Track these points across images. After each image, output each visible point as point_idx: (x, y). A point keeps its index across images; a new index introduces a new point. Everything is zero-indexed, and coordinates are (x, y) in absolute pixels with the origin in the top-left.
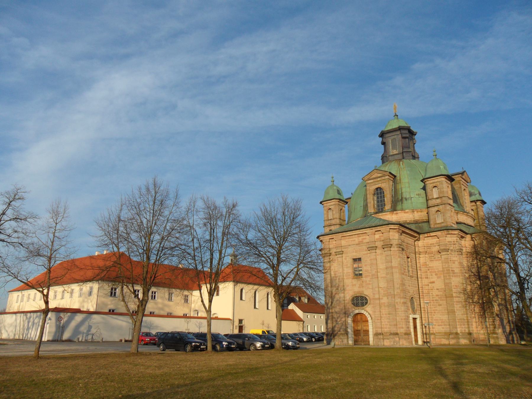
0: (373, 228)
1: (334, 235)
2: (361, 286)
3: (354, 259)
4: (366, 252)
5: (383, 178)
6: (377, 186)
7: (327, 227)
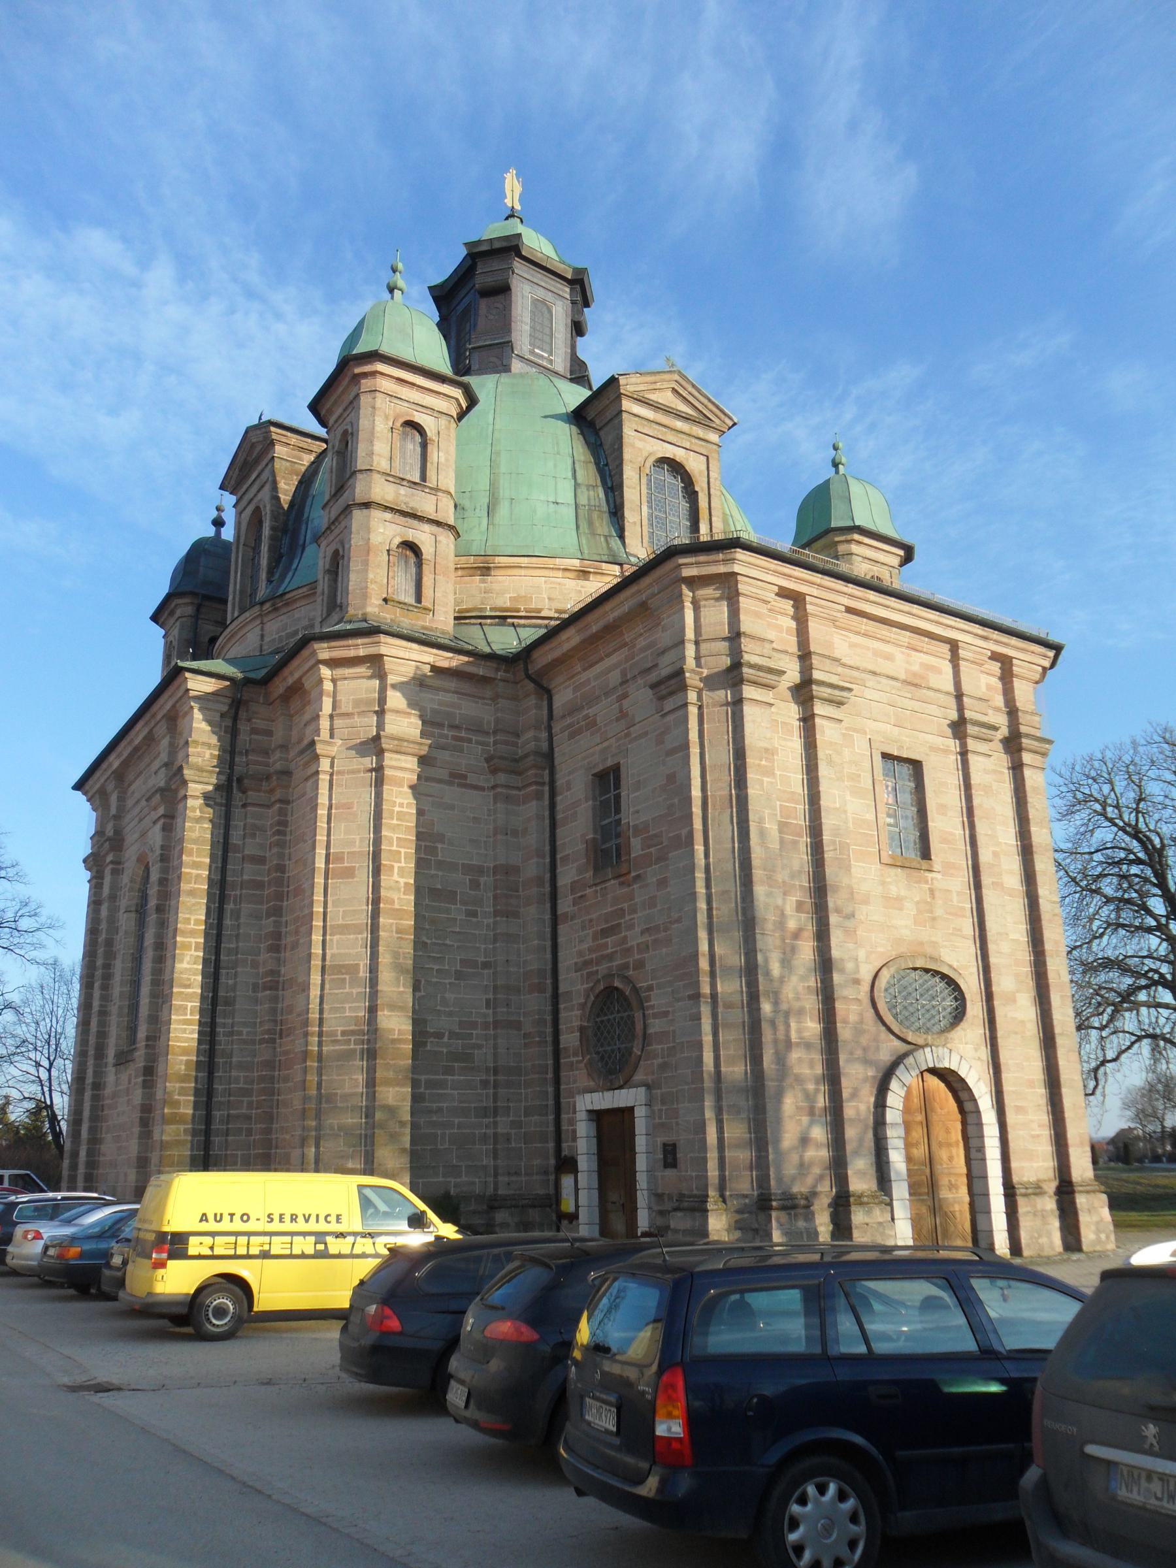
0: (995, 635)
1: (817, 578)
2: (927, 914)
3: (885, 756)
4: (940, 741)
5: (699, 431)
6: (670, 451)
7: (388, 516)
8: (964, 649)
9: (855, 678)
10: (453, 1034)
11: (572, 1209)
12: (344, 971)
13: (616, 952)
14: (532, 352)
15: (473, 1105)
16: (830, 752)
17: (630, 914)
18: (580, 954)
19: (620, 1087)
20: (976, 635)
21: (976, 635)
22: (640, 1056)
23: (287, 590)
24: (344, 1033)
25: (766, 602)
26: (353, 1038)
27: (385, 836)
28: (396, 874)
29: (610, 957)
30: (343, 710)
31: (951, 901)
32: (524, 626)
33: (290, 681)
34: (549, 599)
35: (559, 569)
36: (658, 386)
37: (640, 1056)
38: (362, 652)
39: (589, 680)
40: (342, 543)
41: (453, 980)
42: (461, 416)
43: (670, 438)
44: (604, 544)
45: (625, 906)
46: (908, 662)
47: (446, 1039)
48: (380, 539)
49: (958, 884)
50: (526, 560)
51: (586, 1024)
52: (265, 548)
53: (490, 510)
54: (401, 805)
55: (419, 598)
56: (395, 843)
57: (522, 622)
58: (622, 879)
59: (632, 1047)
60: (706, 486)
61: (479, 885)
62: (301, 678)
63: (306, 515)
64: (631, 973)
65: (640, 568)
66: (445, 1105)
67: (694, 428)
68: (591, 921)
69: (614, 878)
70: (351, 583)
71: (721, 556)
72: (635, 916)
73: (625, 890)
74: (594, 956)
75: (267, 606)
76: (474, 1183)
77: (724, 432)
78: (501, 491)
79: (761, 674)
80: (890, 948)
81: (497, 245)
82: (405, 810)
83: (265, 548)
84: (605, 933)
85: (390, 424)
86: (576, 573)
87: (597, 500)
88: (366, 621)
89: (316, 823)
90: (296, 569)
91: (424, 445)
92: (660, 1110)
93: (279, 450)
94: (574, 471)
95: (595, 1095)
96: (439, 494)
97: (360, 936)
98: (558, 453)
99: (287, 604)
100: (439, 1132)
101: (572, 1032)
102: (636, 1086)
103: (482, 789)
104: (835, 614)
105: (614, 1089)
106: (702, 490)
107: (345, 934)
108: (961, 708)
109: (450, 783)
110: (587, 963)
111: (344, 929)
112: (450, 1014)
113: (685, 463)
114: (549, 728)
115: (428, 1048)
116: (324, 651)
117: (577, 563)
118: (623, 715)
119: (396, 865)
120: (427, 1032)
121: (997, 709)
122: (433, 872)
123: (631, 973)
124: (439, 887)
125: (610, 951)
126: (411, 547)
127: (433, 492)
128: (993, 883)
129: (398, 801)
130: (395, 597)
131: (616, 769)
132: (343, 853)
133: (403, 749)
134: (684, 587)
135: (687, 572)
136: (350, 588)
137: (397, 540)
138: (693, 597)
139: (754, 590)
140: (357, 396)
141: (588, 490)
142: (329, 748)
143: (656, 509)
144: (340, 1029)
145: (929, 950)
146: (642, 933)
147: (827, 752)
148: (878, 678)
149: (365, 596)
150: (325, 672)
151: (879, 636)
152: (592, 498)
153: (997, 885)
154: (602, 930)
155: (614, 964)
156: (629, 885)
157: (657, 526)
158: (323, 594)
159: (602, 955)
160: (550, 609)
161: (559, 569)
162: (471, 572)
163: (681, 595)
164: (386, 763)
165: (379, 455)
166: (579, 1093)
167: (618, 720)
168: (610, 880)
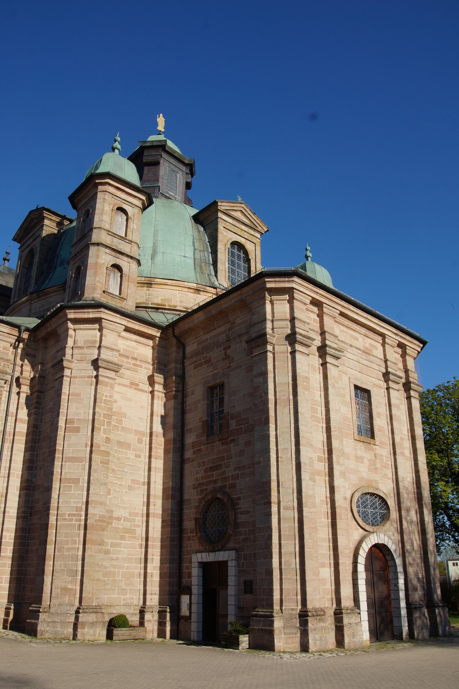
1: (329, 296)
4: (377, 382)
7: (108, 251)
8: (388, 339)
9: (343, 347)
10: (126, 519)
11: (188, 614)
12: (71, 482)
13: (219, 479)
14: (167, 193)
15: (134, 557)
16: (334, 382)
17: (227, 460)
18: (196, 479)
19: (219, 550)
20: (393, 332)
21: (393, 332)
22: (232, 534)
23: (47, 287)
24: (69, 515)
25: (306, 304)
26: (74, 518)
27: (98, 412)
28: (101, 432)
29: (215, 482)
30: (79, 344)
31: (383, 460)
32: (168, 313)
33: (49, 329)
34: (180, 301)
35: (186, 287)
36: (235, 208)
37: (232, 534)
38: (91, 316)
39: (207, 339)
40: (83, 263)
41: (127, 490)
42: (144, 208)
43: (239, 232)
44: (207, 278)
45: (225, 455)
46: (364, 342)
47: (122, 521)
48: (103, 261)
49: (386, 451)
50: (170, 281)
51: (199, 517)
52: (35, 268)
53: (153, 256)
54: (106, 396)
55: (120, 294)
56: (102, 416)
57: (166, 311)
58: (224, 441)
59: (227, 529)
60: (254, 257)
61: (143, 441)
62: (56, 328)
63: (58, 253)
64: (228, 490)
65: (227, 292)
66: (120, 556)
67: (250, 230)
68: (204, 462)
69: (219, 441)
70: (87, 282)
71: (287, 279)
72: (231, 460)
73: (225, 447)
74: (205, 481)
75: (35, 295)
76: (133, 598)
77: (263, 234)
78: (158, 249)
79: (305, 339)
80: (358, 482)
81: (155, 144)
82: (108, 399)
83: (35, 268)
84: (212, 469)
85: (112, 208)
86: (194, 290)
87: (204, 257)
88: (94, 300)
89: (60, 402)
90: (51, 278)
91: (127, 220)
92: (243, 563)
93: (46, 222)
94: (194, 243)
95: (204, 554)
96: (133, 244)
97: (81, 464)
98: (186, 234)
99: (45, 295)
100: (117, 571)
101: (190, 521)
102: (230, 550)
103: (146, 392)
104: (335, 314)
105: (215, 551)
106: (252, 258)
107: (72, 462)
108: (386, 367)
109: (131, 387)
110: (200, 485)
111: (73, 459)
112: (125, 508)
113: (245, 245)
114: (183, 363)
115: (113, 526)
116: (71, 314)
117: (195, 285)
118: (227, 357)
119: (102, 427)
120: (113, 517)
121: (400, 369)
122: (120, 433)
123: (228, 490)
124: (122, 441)
125: (215, 478)
126: (117, 267)
127: (130, 242)
128: (401, 452)
129: (105, 394)
130: (108, 291)
131: (222, 386)
132: (74, 419)
133: (109, 367)
134: (266, 293)
135: (269, 285)
136: (86, 284)
137: (111, 263)
138: (271, 299)
139: (301, 298)
140: (96, 194)
141: (200, 252)
142: (70, 364)
143: (231, 265)
144: (67, 513)
145: (374, 485)
146: (235, 469)
147: (333, 381)
148: (352, 348)
149: (94, 289)
150: (70, 325)
151: (352, 328)
152: (202, 256)
153: (403, 454)
154: (210, 467)
155: (217, 485)
156: (228, 444)
157: (231, 273)
158: (70, 287)
159: (210, 480)
160: (181, 307)
161: (186, 287)
162: (142, 285)
163: (264, 297)
164: (100, 373)
165: (105, 222)
166: (193, 553)
167: (224, 359)
168: (217, 441)
